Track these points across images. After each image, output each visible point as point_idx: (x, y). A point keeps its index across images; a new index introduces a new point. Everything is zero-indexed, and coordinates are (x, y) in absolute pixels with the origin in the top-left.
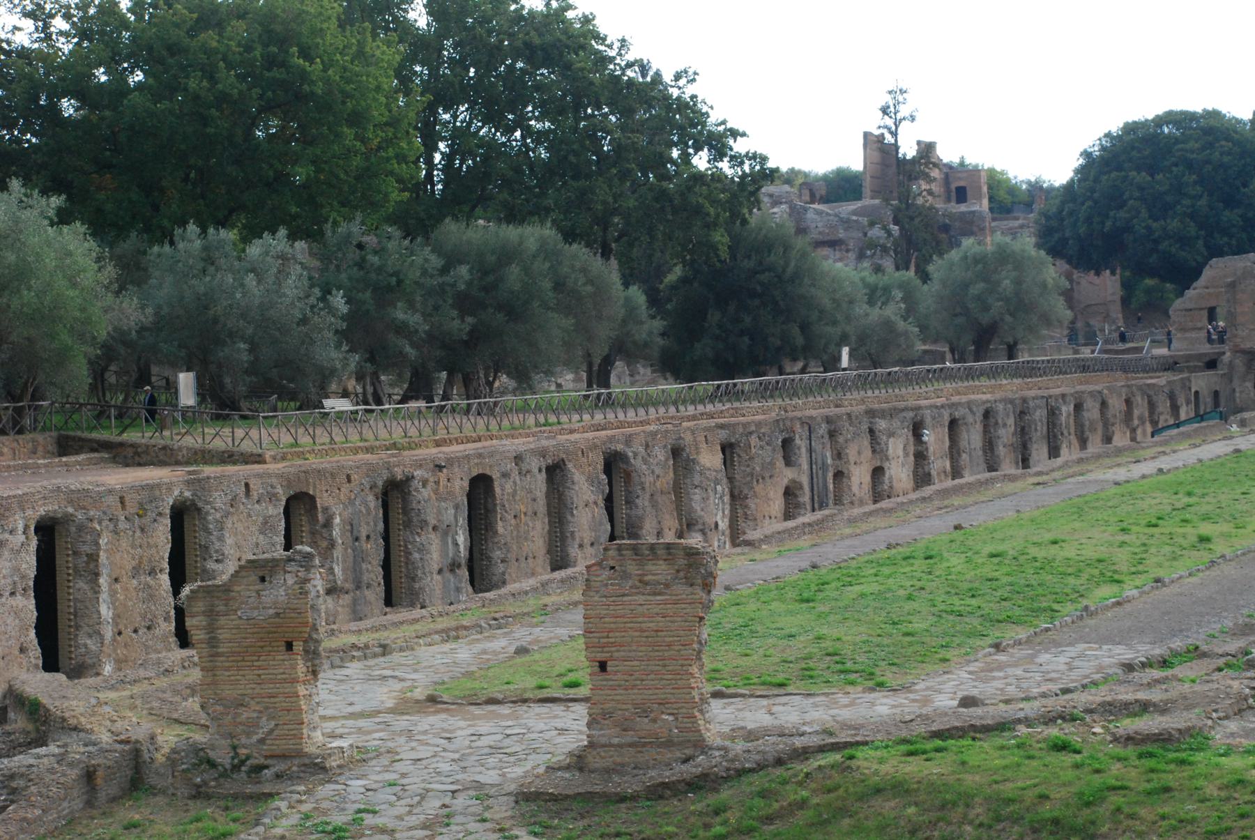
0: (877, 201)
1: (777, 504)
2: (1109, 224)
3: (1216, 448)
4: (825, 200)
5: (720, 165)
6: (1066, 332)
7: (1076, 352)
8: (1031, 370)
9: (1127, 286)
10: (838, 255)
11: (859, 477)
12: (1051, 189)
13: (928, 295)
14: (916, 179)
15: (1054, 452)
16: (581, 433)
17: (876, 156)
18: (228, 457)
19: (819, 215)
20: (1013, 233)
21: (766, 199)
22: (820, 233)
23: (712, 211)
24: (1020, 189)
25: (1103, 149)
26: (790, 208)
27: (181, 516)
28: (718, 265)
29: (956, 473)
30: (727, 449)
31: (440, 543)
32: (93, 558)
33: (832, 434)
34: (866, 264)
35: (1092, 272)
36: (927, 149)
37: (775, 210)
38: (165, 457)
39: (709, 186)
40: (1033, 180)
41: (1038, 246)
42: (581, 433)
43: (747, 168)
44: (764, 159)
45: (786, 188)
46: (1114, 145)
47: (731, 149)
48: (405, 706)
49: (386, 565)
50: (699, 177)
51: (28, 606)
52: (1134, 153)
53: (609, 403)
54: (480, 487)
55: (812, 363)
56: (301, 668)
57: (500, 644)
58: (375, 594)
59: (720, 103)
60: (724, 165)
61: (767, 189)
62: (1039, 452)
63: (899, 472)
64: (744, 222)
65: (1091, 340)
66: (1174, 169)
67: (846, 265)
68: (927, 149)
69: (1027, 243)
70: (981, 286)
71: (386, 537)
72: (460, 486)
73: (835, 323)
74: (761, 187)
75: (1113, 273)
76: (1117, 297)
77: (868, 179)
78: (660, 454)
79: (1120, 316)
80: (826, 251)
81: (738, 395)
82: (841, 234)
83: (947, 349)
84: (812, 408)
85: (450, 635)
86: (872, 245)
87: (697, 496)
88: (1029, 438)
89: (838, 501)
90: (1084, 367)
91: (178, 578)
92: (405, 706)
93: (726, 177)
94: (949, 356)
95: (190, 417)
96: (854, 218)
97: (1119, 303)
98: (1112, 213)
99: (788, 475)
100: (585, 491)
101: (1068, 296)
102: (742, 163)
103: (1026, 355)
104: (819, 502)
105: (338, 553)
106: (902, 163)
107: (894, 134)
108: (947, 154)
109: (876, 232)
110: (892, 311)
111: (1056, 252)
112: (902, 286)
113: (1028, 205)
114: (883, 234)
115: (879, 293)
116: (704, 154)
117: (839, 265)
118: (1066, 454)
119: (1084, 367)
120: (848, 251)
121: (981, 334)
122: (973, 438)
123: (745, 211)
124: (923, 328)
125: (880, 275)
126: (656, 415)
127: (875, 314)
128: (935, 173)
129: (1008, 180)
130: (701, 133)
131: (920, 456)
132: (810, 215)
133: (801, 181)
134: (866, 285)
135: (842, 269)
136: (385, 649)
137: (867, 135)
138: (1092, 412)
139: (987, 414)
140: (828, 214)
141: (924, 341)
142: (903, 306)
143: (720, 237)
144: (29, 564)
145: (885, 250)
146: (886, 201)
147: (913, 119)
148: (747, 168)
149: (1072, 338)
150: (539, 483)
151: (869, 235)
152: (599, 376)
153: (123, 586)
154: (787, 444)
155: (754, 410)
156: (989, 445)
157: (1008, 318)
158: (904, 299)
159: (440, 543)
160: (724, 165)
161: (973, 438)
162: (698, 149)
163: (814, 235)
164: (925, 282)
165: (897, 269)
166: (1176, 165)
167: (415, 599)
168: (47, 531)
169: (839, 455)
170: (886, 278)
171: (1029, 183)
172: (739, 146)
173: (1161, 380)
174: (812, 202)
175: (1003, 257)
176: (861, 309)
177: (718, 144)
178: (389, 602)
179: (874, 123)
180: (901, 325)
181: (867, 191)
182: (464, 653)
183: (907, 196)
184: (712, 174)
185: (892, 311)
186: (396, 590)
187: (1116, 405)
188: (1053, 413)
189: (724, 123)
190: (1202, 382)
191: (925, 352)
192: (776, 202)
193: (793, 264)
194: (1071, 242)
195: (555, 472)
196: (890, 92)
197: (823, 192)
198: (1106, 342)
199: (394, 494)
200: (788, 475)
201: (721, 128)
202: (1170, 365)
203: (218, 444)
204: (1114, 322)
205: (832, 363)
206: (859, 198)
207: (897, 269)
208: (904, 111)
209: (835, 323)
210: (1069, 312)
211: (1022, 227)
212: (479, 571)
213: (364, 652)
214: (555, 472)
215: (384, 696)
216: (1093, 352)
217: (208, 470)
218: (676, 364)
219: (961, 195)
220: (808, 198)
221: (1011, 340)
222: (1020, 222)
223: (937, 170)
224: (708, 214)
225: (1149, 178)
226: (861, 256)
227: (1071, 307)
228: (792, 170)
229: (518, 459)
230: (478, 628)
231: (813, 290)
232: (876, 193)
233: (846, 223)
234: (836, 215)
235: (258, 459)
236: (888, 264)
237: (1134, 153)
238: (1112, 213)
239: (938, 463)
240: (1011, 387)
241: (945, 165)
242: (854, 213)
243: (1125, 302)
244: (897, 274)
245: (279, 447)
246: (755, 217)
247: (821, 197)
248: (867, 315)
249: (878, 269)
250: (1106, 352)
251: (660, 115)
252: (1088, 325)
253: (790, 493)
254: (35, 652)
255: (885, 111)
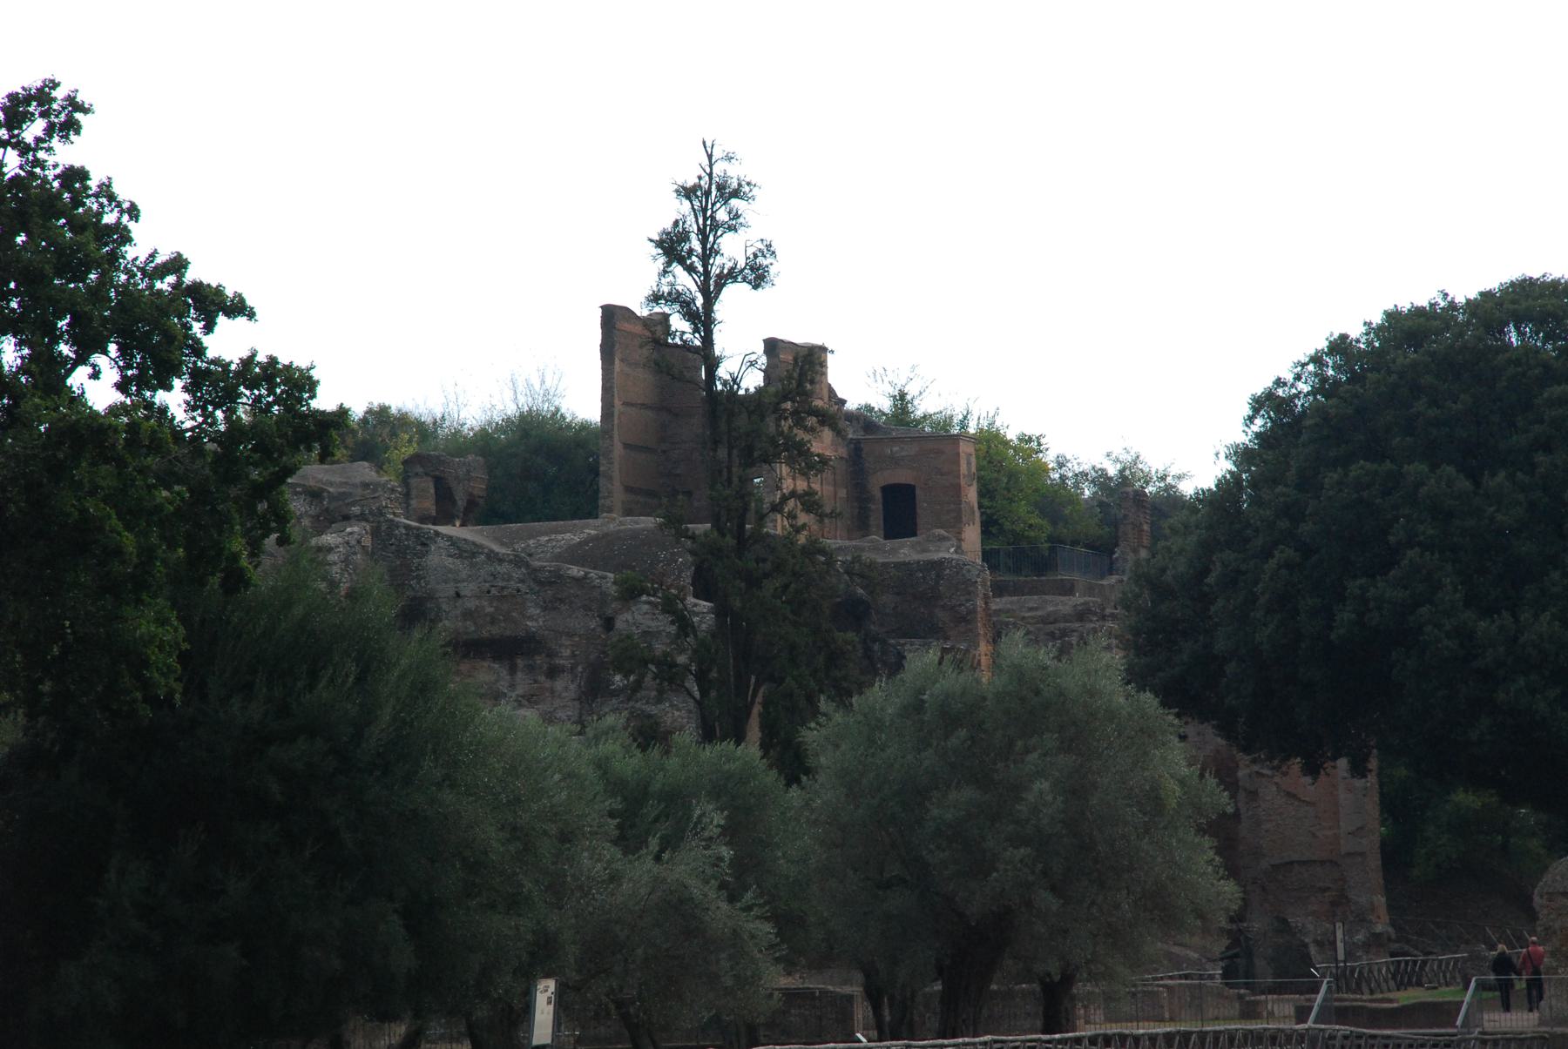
0: (648, 522)
2: (1345, 615)
4: (486, 512)
5: (161, 397)
6: (1219, 946)
7: (1249, 1012)
9: (1394, 806)
10: (523, 683)
12: (1170, 502)
13: (802, 819)
14: (767, 460)
17: (642, 383)
19: (464, 557)
20: (1059, 635)
21: (297, 505)
22: (468, 614)
23: (129, 541)
24: (1074, 499)
25: (1324, 387)
26: (375, 533)
28: (146, 712)
34: (613, 718)
35: (1296, 763)
36: (798, 367)
37: (329, 539)
39: (121, 463)
40: (1112, 471)
41: (1137, 677)
43: (243, 413)
44: (301, 383)
45: (364, 471)
46: (1354, 378)
47: (199, 350)
50: (89, 432)
52: (1420, 405)
55: (435, 1028)
60: (174, 399)
61: (312, 472)
64: (236, 580)
65: (1293, 973)
66: (1540, 457)
67: (549, 719)
69: (1101, 668)
70: (967, 794)
73: (515, 903)
74: (290, 471)
75: (1359, 770)
76: (1370, 844)
77: (618, 450)
79: (1380, 900)
80: (486, 673)
82: (535, 620)
83: (855, 989)
86: (631, 657)
93: (177, 434)
94: (861, 1012)
96: (576, 571)
97: (1375, 861)
98: (1354, 586)
101: (1225, 833)
102: (228, 398)
103: (1099, 1015)
106: (726, 405)
107: (704, 321)
109: (640, 618)
110: (692, 869)
111: (1185, 696)
112: (725, 789)
113: (1102, 550)
114: (664, 624)
115: (651, 809)
116: (107, 363)
117: (530, 715)
120: (553, 672)
123: (237, 545)
124: (787, 922)
125: (655, 753)
127: (641, 873)
128: (823, 444)
129: (1043, 469)
130: (97, 294)
132: (437, 558)
133: (408, 451)
134: (616, 786)
135: (533, 730)
137: (612, 316)
140: (492, 557)
141: (790, 965)
142: (726, 852)
143: (155, 626)
145: (670, 675)
146: (674, 522)
147: (757, 275)
148: (243, 413)
149: (1237, 966)
151: (619, 624)
157: (1046, 900)
158: (730, 832)
160: (174, 399)
162: (88, 346)
163: (449, 624)
164: (793, 779)
165: (708, 735)
166: (1547, 448)
170: (673, 762)
171: (1101, 479)
172: (226, 342)
174: (445, 517)
175: (1033, 710)
176: (596, 858)
179: (636, 281)
180: (721, 914)
181: (613, 489)
184: (133, 427)
185: (692, 869)
189: (177, 264)
191: (791, 996)
192: (331, 517)
193: (386, 714)
194: (1231, 668)
196: (688, 193)
197: (479, 488)
198: (1343, 980)
201: (165, 285)
204: (1362, 919)
206: (586, 505)
207: (708, 735)
208: (732, 249)
209: (515, 903)
210: (1230, 888)
211: (1081, 615)
216: (1302, 1014)
220: (429, 505)
221: (1054, 968)
222: (1078, 599)
223: (827, 434)
224: (118, 552)
225: (1465, 484)
226: (594, 691)
227: (1233, 872)
228: (380, 416)
231: (448, 796)
232: (642, 498)
233: (550, 586)
234: (518, 562)
236: (678, 714)
237: (1420, 405)
238: (1354, 586)
241: (853, 417)
242: (575, 555)
243: (1394, 858)
244: (709, 753)
246: (267, 568)
247: (472, 503)
248: (615, 878)
249: (649, 735)
250: (1342, 1015)
252: (1283, 926)
255: (671, 246)
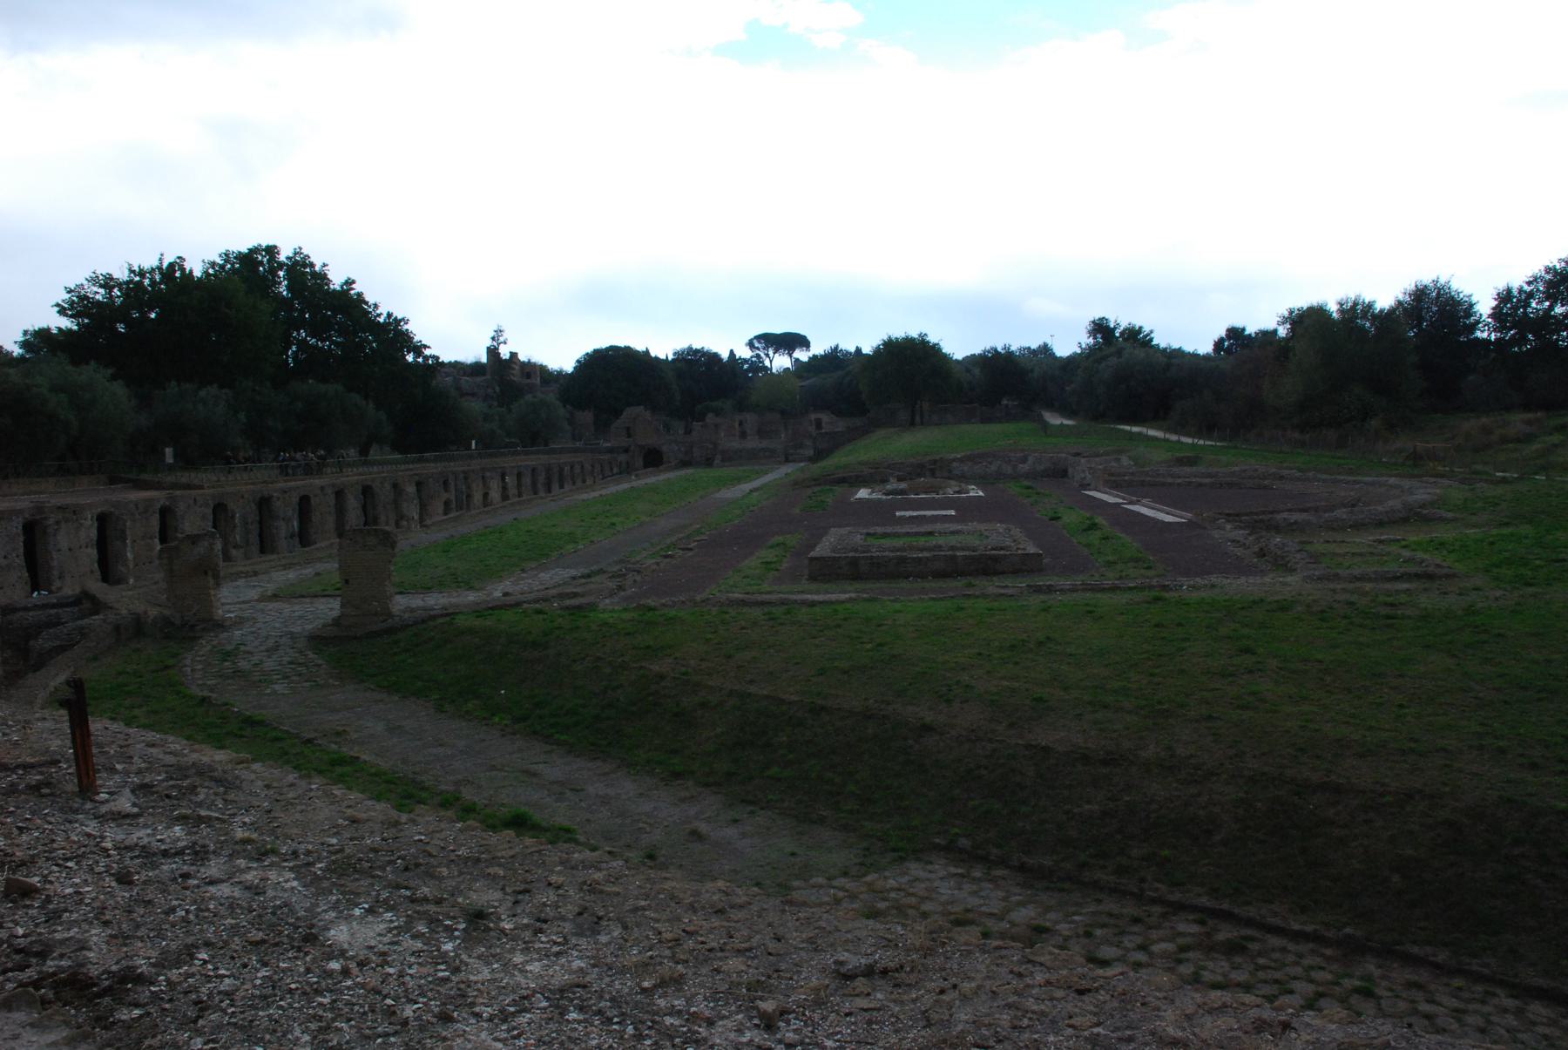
1: (441, 509)
3: (626, 486)
8: (553, 451)
11: (477, 497)
15: (562, 487)
16: (352, 477)
18: (188, 487)
27: (165, 513)
29: (520, 495)
30: (418, 484)
31: (286, 525)
32: (123, 531)
33: (466, 478)
36: (514, 355)
38: (158, 486)
42: (352, 477)
48: (263, 598)
49: (260, 535)
51: (94, 552)
53: (365, 463)
54: (304, 501)
56: (212, 582)
57: (308, 571)
58: (255, 548)
59: (419, 330)
62: (555, 486)
63: (495, 495)
68: (514, 355)
71: (260, 523)
72: (295, 500)
78: (388, 486)
81: (427, 461)
84: (457, 467)
85: (285, 567)
87: (405, 505)
88: (552, 480)
89: (468, 508)
90: (576, 450)
91: (163, 540)
92: (263, 598)
95: (171, 468)
99: (445, 496)
100: (353, 504)
104: (459, 508)
105: (238, 530)
108: (522, 357)
118: (567, 487)
119: (576, 450)
121: (534, 435)
122: (527, 480)
126: (387, 468)
131: (504, 488)
135: (475, 406)
136: (256, 574)
138: (577, 470)
139: (533, 470)
144: (94, 533)
150: (332, 500)
152: (364, 451)
153: (139, 545)
154: (446, 483)
155: (432, 468)
156: (534, 484)
159: (286, 525)
161: (527, 480)
167: (273, 551)
168: (102, 520)
169: (469, 487)
172: (427, 352)
173: (607, 457)
177: (418, 349)
178: (263, 551)
179: (489, 343)
182: (291, 575)
183: (503, 376)
186: (266, 545)
187: (588, 467)
188: (561, 470)
190: (622, 458)
195: (339, 494)
199: (264, 503)
200: (445, 496)
202: (611, 450)
203: (184, 480)
205: (469, 447)
212: (304, 538)
213: (247, 575)
214: (339, 494)
215: (253, 594)
217: (178, 493)
218: (398, 447)
219: (528, 376)
229: (322, 488)
230: (299, 564)
235: (201, 487)
239: (512, 491)
240: (544, 458)
245: (210, 482)
251: (394, 336)
253: (447, 503)
254: (98, 574)
